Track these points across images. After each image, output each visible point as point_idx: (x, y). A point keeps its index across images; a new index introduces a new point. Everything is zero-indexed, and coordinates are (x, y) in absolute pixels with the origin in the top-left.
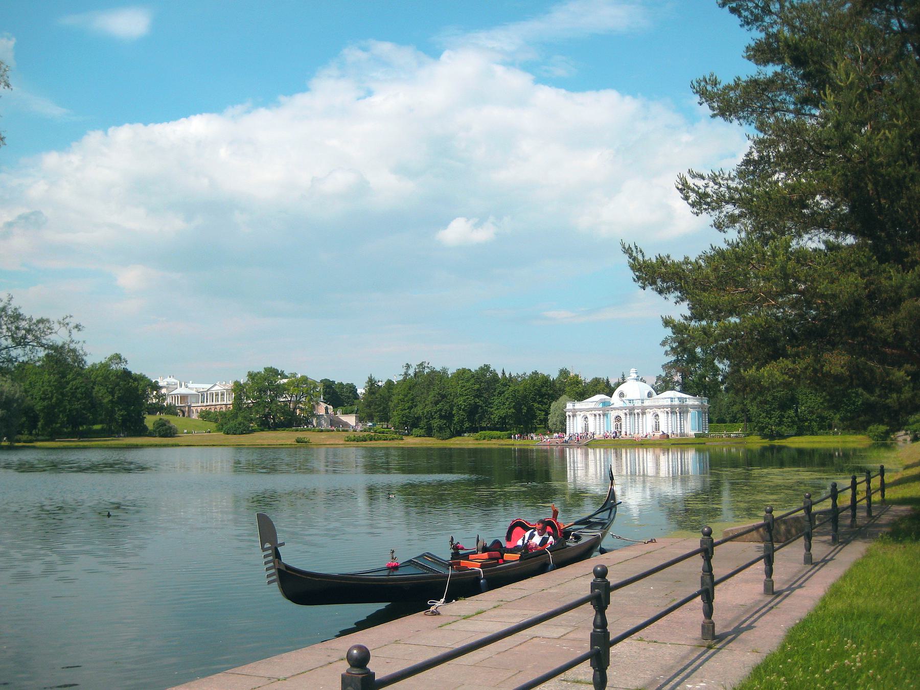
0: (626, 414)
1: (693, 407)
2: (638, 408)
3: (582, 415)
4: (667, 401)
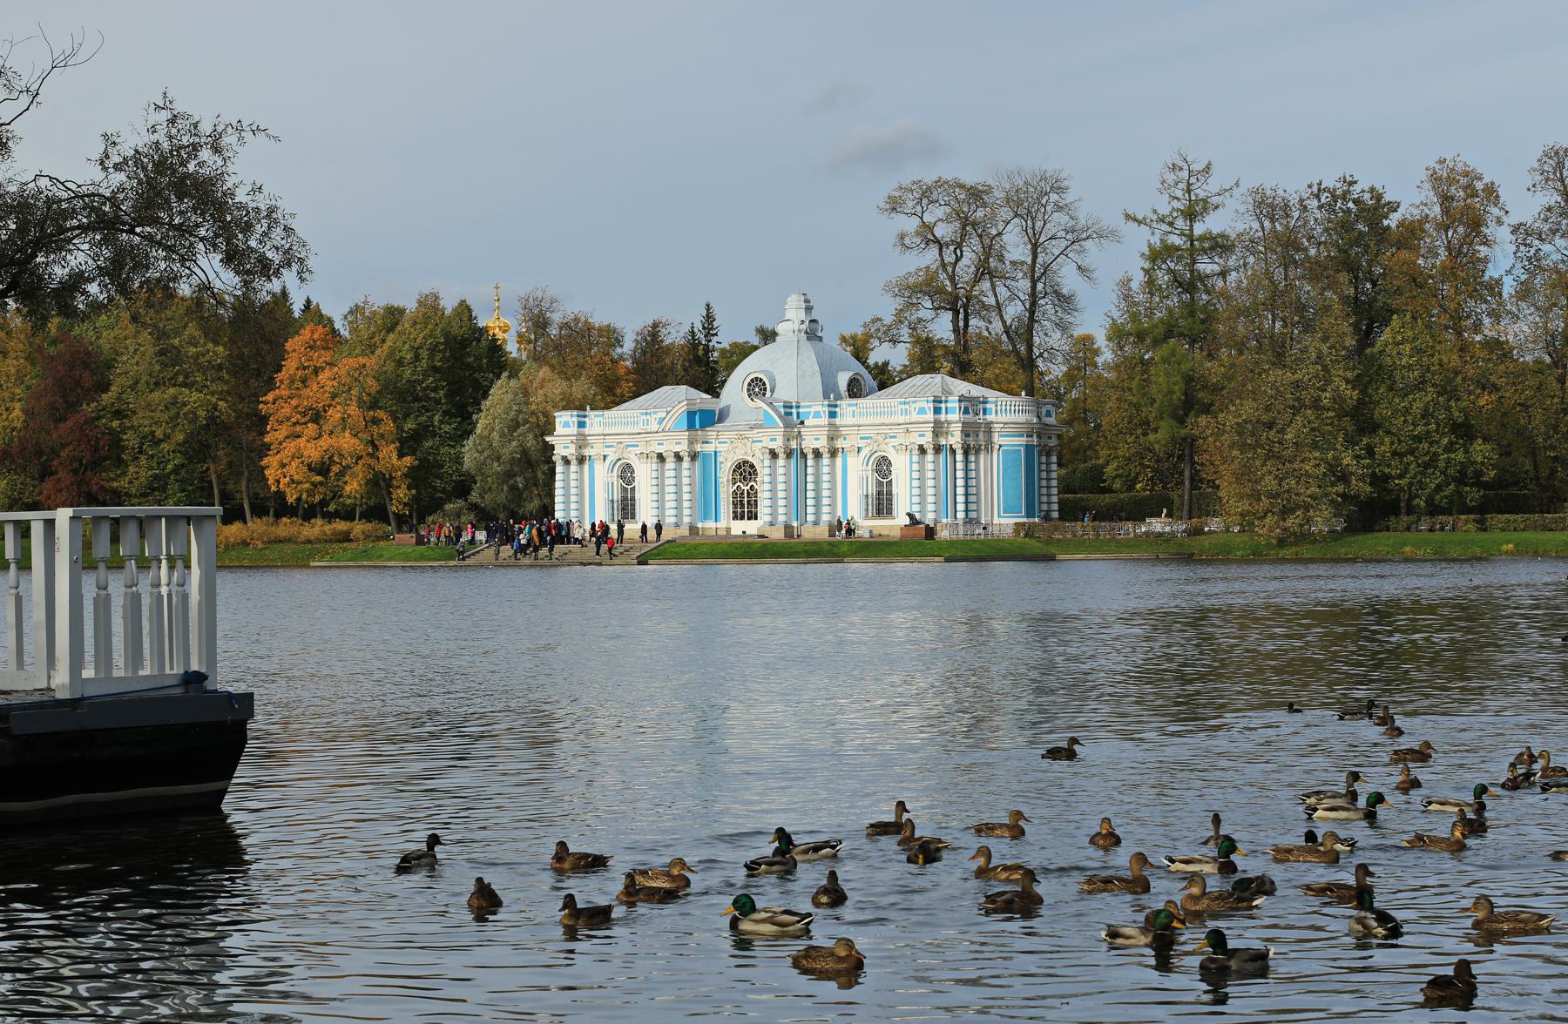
3: (612, 457)
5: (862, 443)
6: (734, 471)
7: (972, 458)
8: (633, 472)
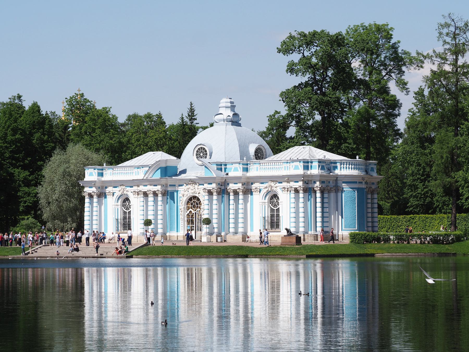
0: (210, 193)
1: (350, 180)
2: (236, 180)
3: (118, 194)
4: (296, 168)
6: (188, 202)
7: (326, 195)
8: (130, 202)
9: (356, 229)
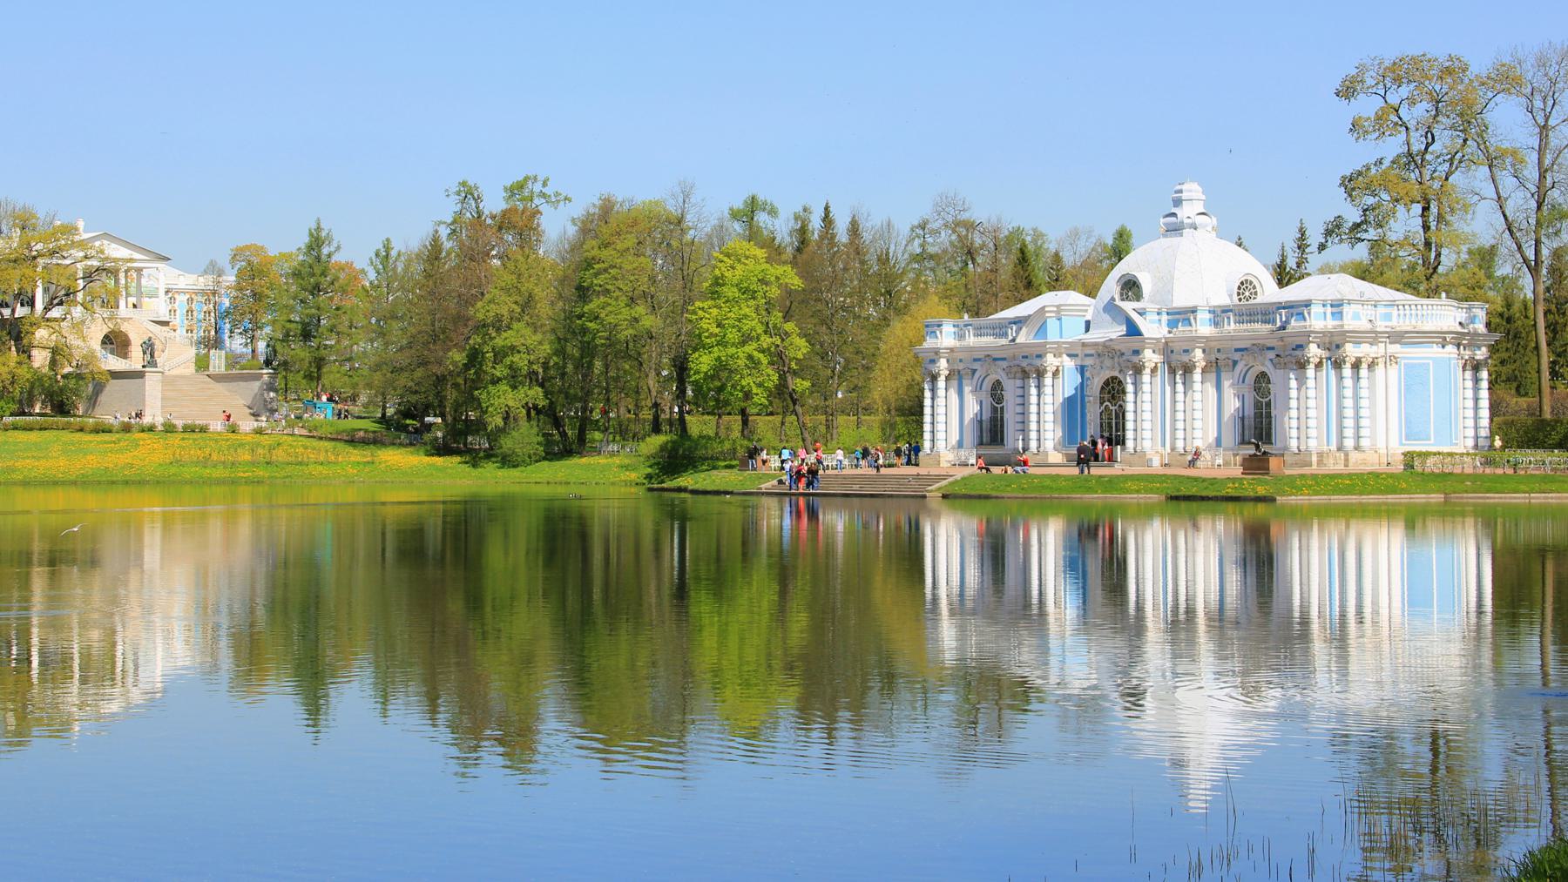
5: (1237, 356)
6: (1102, 388)
7: (1364, 372)
9: (1432, 442)
